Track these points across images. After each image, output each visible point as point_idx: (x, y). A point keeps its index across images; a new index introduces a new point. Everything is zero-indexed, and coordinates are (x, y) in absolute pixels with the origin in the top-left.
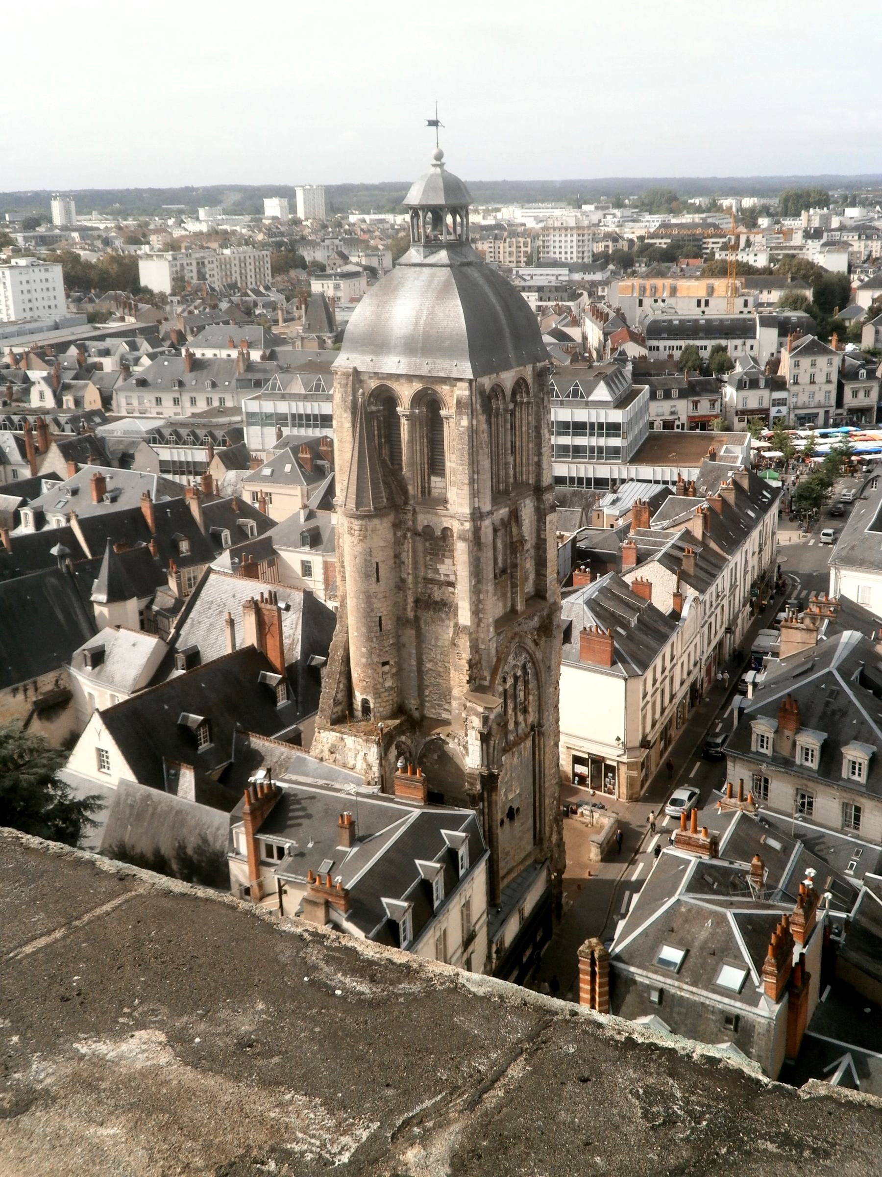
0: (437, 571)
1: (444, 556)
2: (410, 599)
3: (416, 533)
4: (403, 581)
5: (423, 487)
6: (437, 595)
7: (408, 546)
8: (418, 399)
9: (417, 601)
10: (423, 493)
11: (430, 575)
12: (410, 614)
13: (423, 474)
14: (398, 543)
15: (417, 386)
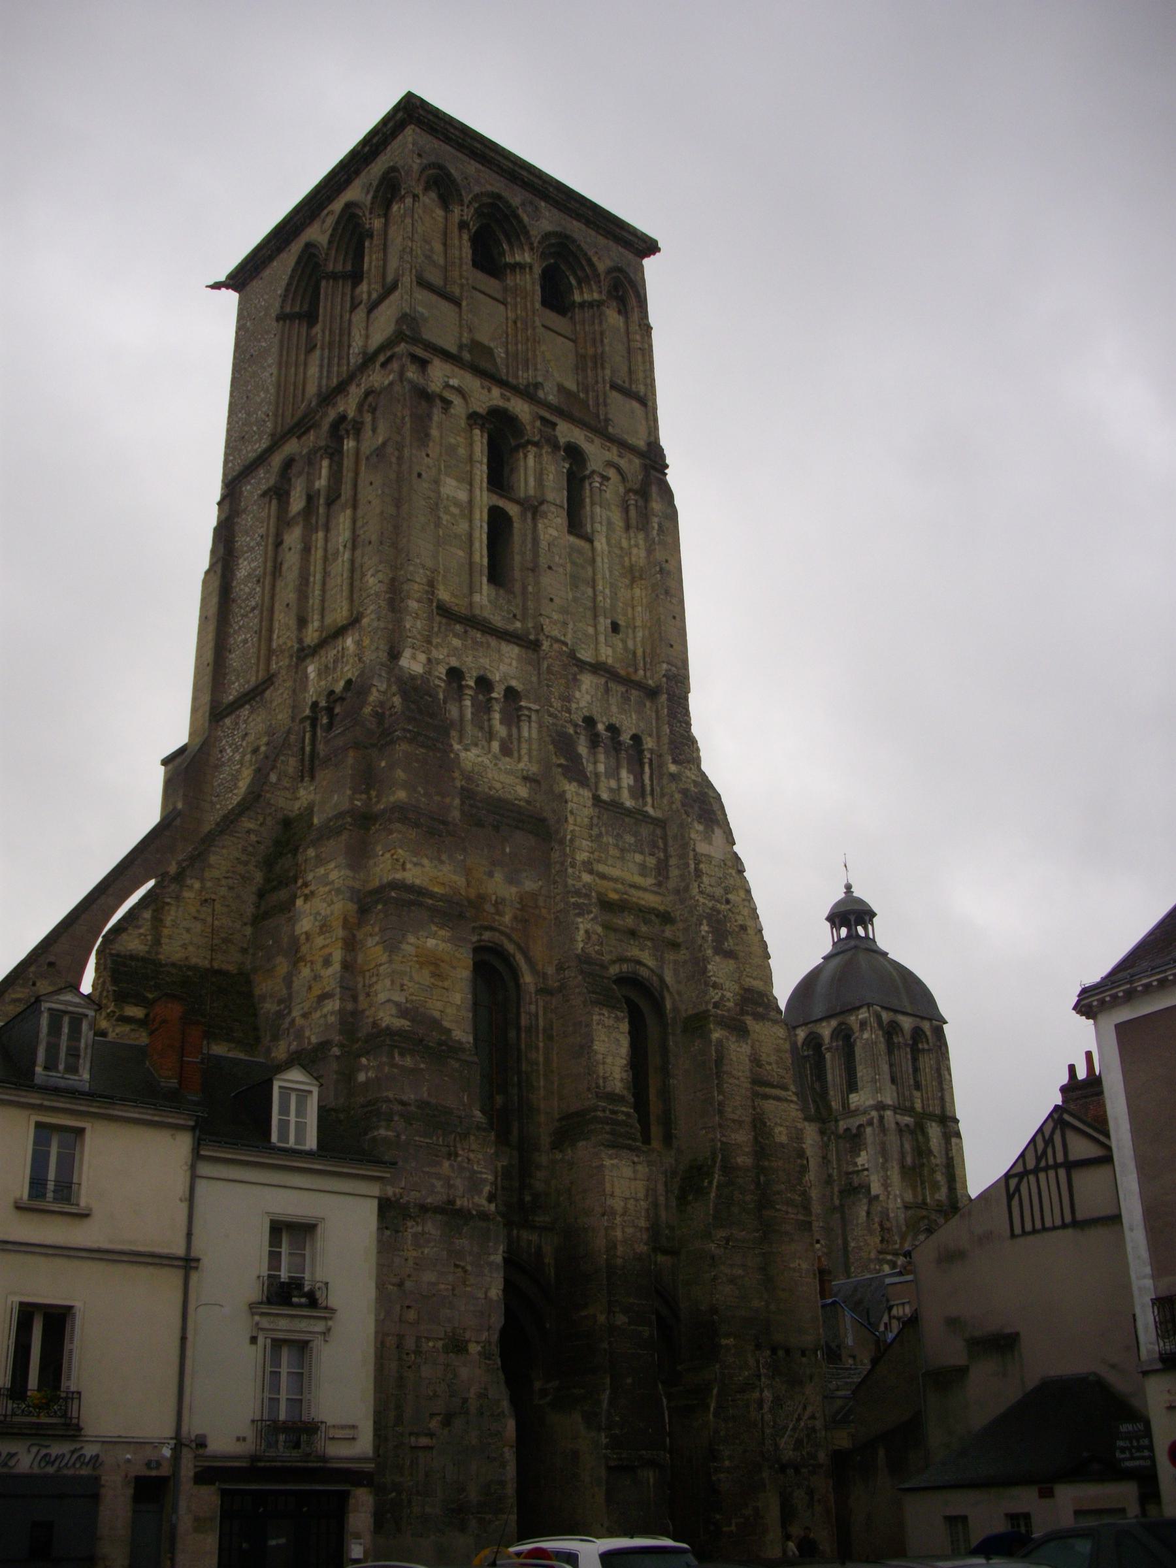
0: (856, 1164)
1: (860, 1150)
2: (836, 1189)
3: (838, 1137)
4: (830, 1176)
5: (843, 1104)
6: (856, 1181)
7: (832, 1146)
8: (835, 1034)
9: (841, 1192)
10: (844, 1107)
11: (851, 1169)
12: (837, 1202)
13: (842, 1092)
14: (825, 1146)
15: (834, 1023)
